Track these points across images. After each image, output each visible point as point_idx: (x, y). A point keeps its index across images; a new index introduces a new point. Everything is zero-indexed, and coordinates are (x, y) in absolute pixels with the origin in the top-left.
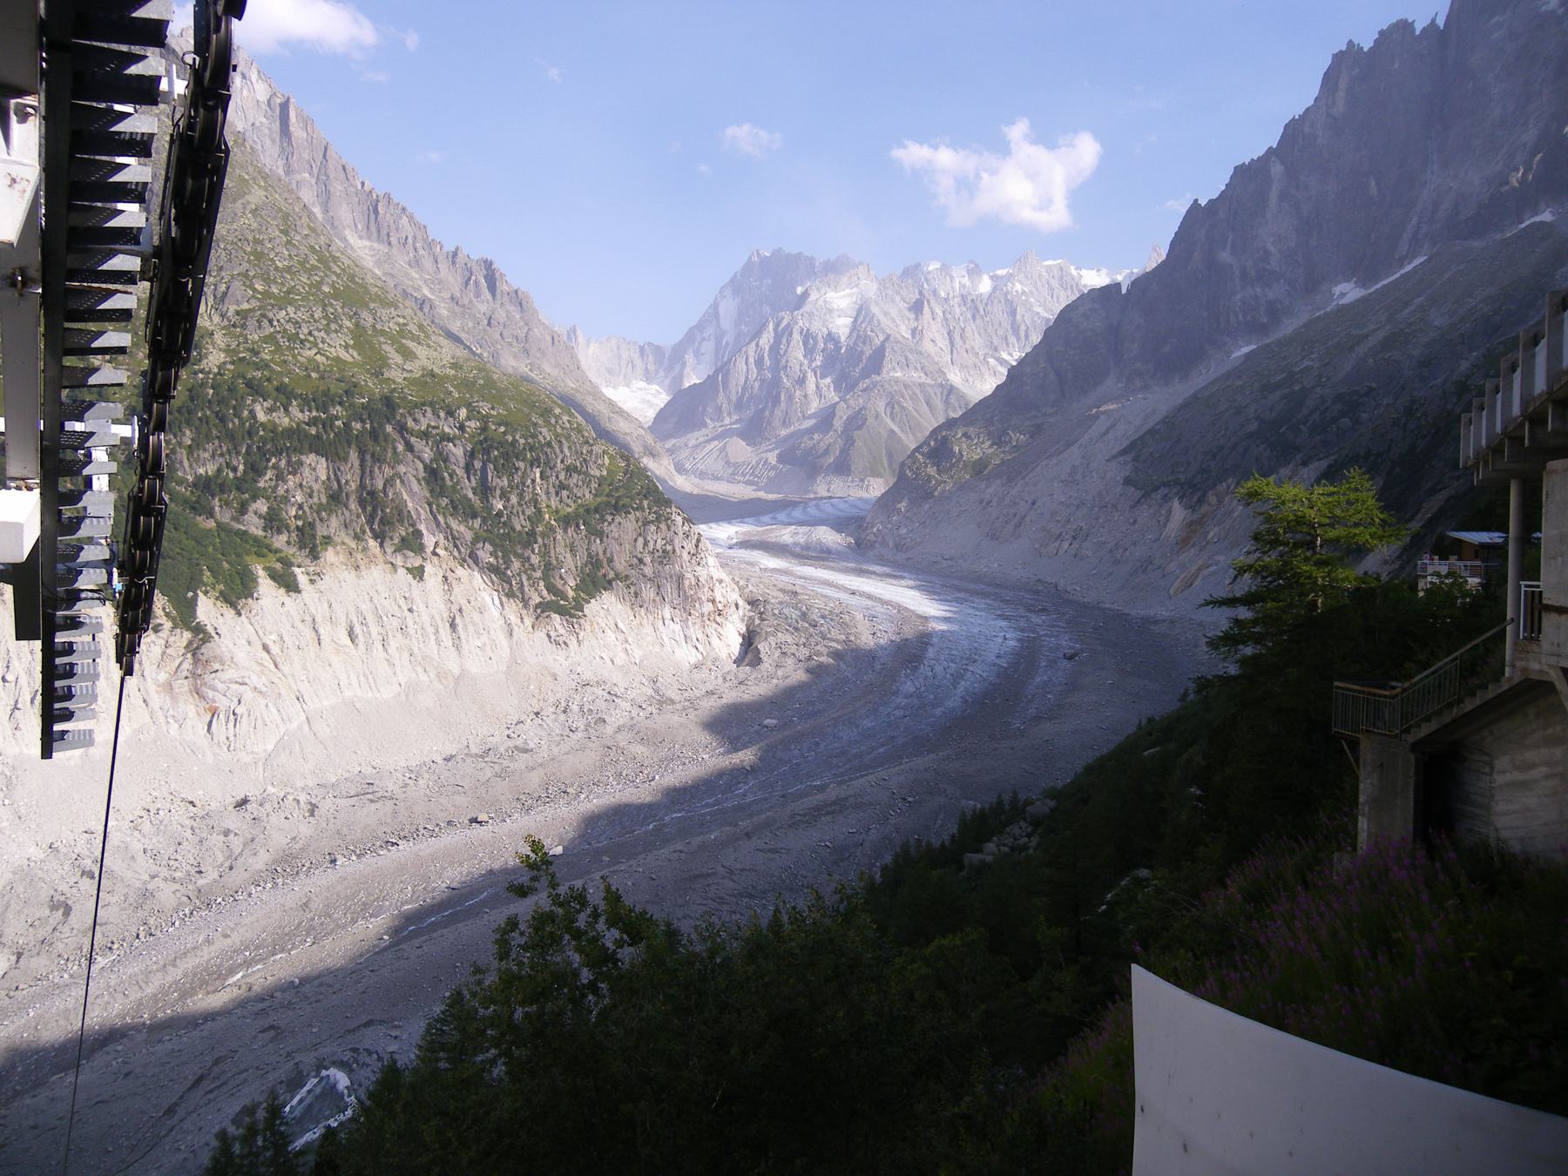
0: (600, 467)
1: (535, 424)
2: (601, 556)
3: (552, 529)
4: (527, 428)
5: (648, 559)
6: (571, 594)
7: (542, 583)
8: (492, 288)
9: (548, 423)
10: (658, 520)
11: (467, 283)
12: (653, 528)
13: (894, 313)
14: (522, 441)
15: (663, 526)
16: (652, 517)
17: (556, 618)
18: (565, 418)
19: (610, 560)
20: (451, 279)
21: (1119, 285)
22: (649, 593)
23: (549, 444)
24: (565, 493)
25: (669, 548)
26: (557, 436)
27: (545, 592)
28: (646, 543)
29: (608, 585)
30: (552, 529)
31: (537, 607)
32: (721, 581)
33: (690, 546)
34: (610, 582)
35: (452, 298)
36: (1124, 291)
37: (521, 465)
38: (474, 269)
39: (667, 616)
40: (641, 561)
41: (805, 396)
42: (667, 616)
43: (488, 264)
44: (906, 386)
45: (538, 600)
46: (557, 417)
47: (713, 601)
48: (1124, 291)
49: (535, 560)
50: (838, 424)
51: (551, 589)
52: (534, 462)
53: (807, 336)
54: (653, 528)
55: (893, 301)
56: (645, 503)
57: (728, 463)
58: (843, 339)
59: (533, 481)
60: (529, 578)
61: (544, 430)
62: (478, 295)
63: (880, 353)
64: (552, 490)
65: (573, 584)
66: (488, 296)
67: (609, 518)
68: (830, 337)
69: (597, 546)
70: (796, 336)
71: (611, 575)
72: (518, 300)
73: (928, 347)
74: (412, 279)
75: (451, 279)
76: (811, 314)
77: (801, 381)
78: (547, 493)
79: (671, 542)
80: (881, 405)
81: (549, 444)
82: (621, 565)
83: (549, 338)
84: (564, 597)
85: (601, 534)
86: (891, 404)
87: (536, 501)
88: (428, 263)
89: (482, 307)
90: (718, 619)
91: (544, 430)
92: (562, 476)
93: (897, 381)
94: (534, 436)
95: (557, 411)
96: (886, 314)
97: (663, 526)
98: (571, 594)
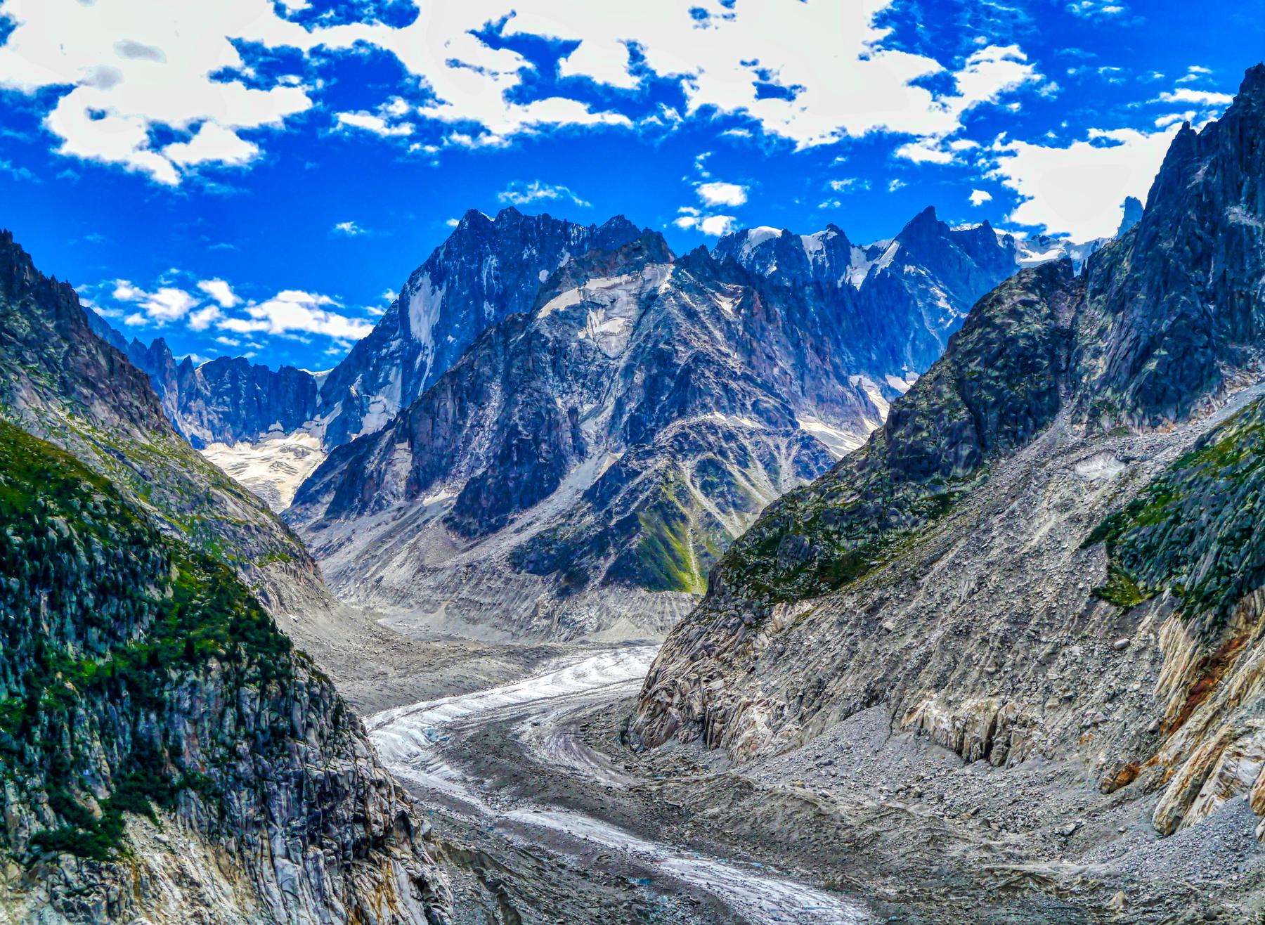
0: (161, 587)
1: (45, 511)
2: (158, 741)
3: (69, 700)
4: (28, 517)
5: (243, 747)
6: (99, 813)
7: (45, 796)
9: (66, 508)
10: (265, 677)
12: (252, 690)
13: (700, 308)
14: (17, 540)
15: (273, 688)
16: (253, 671)
17: (68, 859)
18: (99, 498)
19: (176, 752)
22: (243, 804)
23: (67, 545)
24: (94, 633)
25: (283, 724)
26: (83, 530)
27: (49, 813)
28: (240, 720)
29: (169, 799)
30: (69, 700)
31: (36, 839)
32: (379, 784)
33: (325, 722)
34: (174, 791)
37: (14, 582)
39: (279, 849)
40: (233, 751)
42: (279, 849)
44: (730, 437)
45: (37, 827)
46: (85, 497)
47: (364, 821)
49: (34, 754)
51: (62, 806)
52: (38, 580)
54: (252, 690)
56: (242, 648)
57: (422, 570)
59: (35, 611)
60: (21, 787)
61: (60, 520)
64: (69, 627)
65: (103, 794)
67: (174, 675)
69: (149, 723)
71: (177, 778)
78: (61, 634)
79: (288, 713)
80: (687, 467)
81: (67, 545)
82: (193, 756)
83: (103, 362)
84: (89, 825)
85: (159, 705)
86: (703, 468)
87: (40, 650)
90: (375, 855)
91: (60, 520)
92: (90, 600)
94: (41, 532)
95: (86, 485)
96: (691, 315)
97: (273, 688)
98: (99, 813)
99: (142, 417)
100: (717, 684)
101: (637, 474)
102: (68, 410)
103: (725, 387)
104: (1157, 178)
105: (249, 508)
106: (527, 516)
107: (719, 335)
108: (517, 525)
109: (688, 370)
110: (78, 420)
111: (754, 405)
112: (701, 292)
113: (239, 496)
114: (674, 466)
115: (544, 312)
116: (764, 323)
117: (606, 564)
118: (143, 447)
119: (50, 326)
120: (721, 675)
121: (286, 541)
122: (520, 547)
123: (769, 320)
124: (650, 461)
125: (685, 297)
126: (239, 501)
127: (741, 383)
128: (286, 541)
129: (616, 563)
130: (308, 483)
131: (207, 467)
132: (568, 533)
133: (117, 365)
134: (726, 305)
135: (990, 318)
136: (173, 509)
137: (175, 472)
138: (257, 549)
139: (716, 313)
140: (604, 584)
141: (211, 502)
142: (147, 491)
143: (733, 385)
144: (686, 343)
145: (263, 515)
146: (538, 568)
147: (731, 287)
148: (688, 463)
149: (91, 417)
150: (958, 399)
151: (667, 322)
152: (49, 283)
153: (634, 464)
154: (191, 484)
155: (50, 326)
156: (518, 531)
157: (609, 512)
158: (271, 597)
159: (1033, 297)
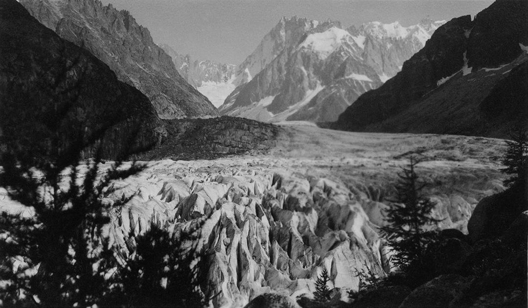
8: (127, 26)
11: (113, 23)
20: (104, 21)
21: (469, 16)
35: (102, 29)
36: (472, 19)
38: (118, 15)
41: (303, 88)
43: (126, 14)
48: (472, 19)
50: (319, 102)
53: (306, 59)
62: (119, 28)
63: (344, 65)
66: (125, 30)
70: (299, 57)
72: (143, 32)
74: (80, 19)
75: (104, 21)
83: (157, 52)
88: (90, 10)
89: (122, 34)
99: (168, 69)
102: (144, 66)
109: (345, 63)
110: (147, 69)
116: (372, 49)
118: (168, 79)
119: (140, 40)
123: (373, 48)
128: (212, 109)
131: (188, 86)
133: (161, 53)
136: (175, 97)
137: (177, 86)
142: (167, 91)
145: (206, 101)
149: (150, 68)
152: (140, 28)
153: (327, 91)
154: (182, 90)
155: (140, 40)
156: (290, 112)
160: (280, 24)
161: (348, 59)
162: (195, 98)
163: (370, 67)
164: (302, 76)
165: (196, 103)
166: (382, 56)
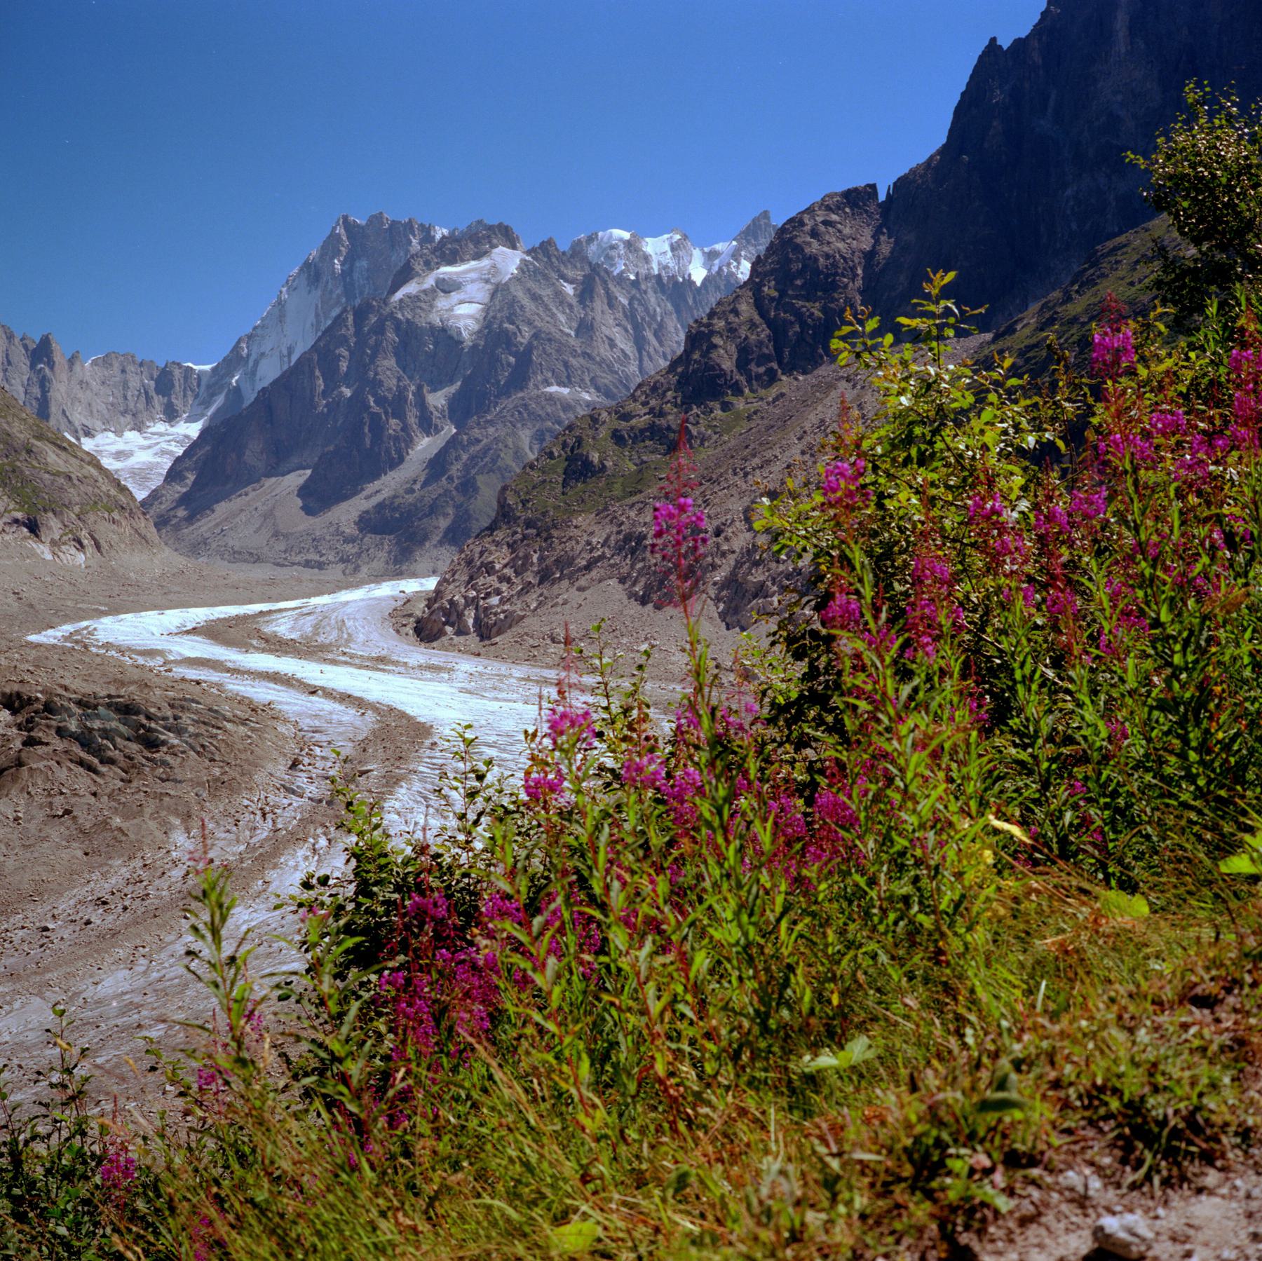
13: (546, 293)
36: (882, 197)
41: (405, 428)
55: (546, 278)
57: (276, 534)
58: (465, 334)
68: (445, 336)
70: (391, 335)
73: (604, 351)
76: (415, 299)
77: (397, 406)
93: (551, 398)
96: (535, 298)
100: (495, 600)
101: (478, 441)
103: (566, 364)
104: (963, 94)
105: (73, 460)
106: (377, 484)
107: (562, 318)
108: (365, 493)
109: (530, 348)
111: (592, 380)
112: (546, 278)
113: (65, 449)
114: (514, 434)
115: (399, 295)
117: (444, 523)
120: (498, 592)
121: (113, 492)
122: (367, 512)
123: (611, 306)
124: (491, 430)
125: (530, 284)
126: (63, 454)
127: (581, 360)
128: (113, 492)
129: (454, 522)
130: (178, 460)
132: (410, 498)
134: (569, 289)
135: (791, 239)
138: (77, 499)
139: (559, 295)
140: (441, 543)
141: (29, 452)
143: (573, 361)
144: (530, 323)
146: (375, 530)
147: (570, 273)
148: (528, 432)
150: (757, 318)
151: (513, 302)
156: (368, 498)
157: (450, 479)
158: (85, 542)
159: (834, 217)
160: (333, 238)
161: (535, 336)
162: (53, 457)
163: (603, 361)
164: (401, 392)
165: (58, 474)
166: (637, 328)
